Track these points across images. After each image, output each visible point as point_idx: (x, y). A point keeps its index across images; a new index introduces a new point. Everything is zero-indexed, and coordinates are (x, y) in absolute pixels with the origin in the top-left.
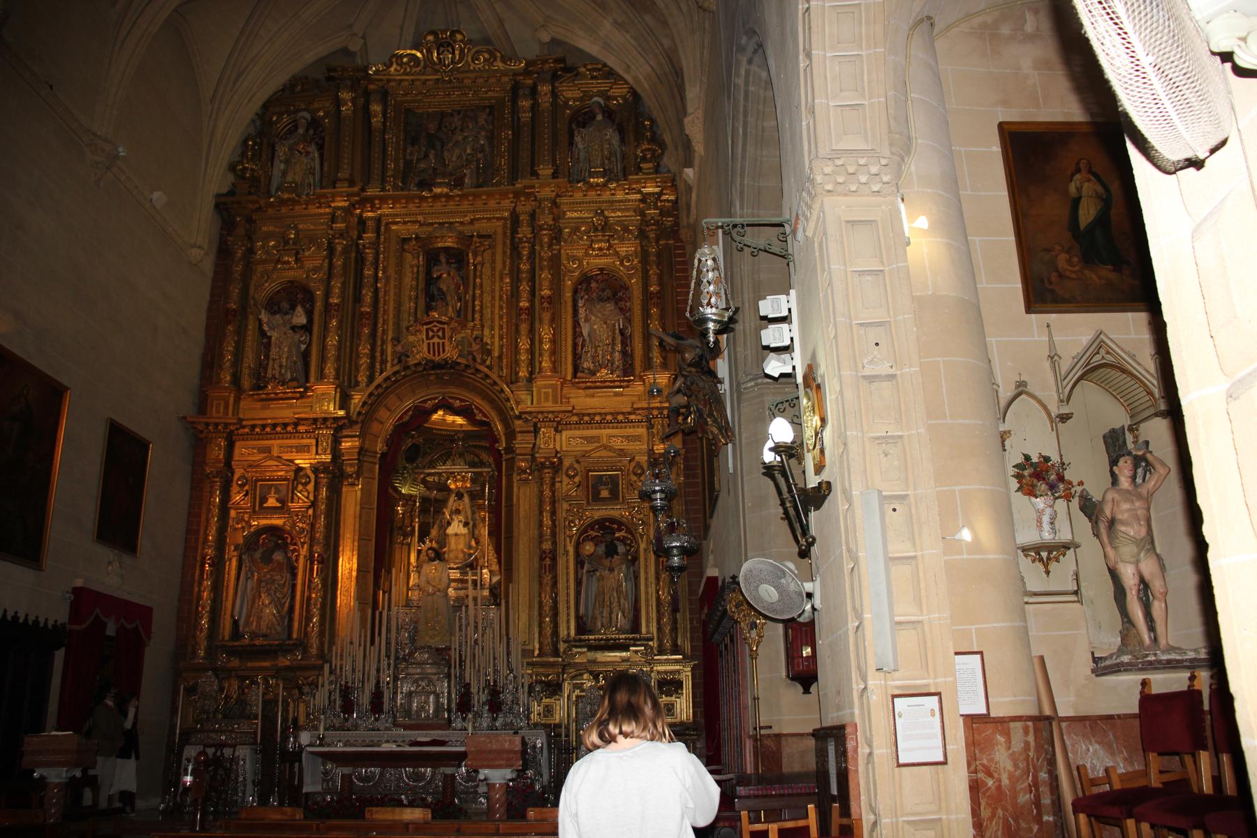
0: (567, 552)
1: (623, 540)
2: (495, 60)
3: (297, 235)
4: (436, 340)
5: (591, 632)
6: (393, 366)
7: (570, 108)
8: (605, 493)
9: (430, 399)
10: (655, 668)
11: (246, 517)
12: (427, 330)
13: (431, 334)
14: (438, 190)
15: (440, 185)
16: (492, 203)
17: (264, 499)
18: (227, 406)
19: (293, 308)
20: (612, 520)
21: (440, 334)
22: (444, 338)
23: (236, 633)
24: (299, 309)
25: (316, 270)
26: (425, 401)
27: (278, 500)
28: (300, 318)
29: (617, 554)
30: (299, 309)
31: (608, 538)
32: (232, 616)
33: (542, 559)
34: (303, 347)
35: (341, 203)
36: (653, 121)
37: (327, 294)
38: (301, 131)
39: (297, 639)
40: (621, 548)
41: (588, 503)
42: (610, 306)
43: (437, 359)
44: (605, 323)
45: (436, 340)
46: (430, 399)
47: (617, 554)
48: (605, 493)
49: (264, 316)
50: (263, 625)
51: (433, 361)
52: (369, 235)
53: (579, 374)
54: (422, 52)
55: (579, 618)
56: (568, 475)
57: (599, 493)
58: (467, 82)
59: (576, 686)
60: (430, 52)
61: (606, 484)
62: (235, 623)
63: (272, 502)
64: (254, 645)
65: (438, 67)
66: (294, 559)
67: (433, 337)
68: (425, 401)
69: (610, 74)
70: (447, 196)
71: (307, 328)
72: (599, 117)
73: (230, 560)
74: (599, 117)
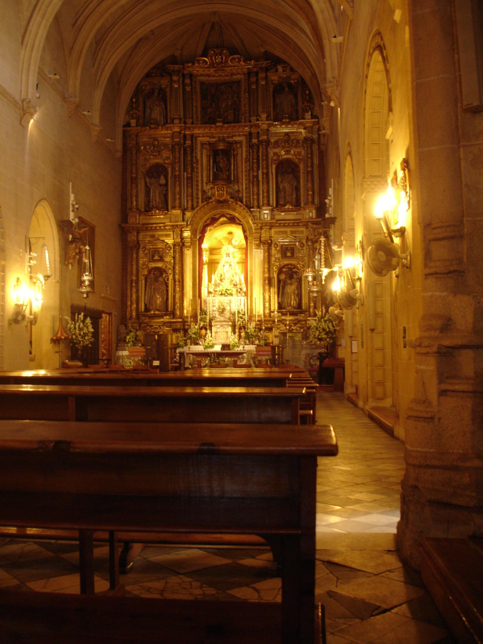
0: (274, 277)
1: (296, 273)
2: (240, 61)
3: (158, 143)
4: (221, 192)
5: (284, 308)
6: (202, 202)
7: (273, 84)
8: (289, 254)
9: (218, 214)
10: (308, 322)
11: (147, 263)
12: (217, 188)
13: (218, 189)
14: (218, 124)
15: (219, 122)
16: (241, 129)
17: (153, 256)
18: (136, 219)
19: (160, 176)
20: (291, 265)
21: (222, 189)
22: (224, 191)
23: (147, 310)
24: (162, 177)
25: (167, 158)
26: (215, 215)
27: (159, 257)
28: (163, 181)
29: (293, 278)
30: (162, 177)
31: (290, 272)
32: (145, 303)
33: (265, 280)
34: (164, 192)
35: (177, 130)
36: (310, 91)
37: (173, 170)
38: (156, 94)
39: (171, 311)
40: (295, 276)
41: (282, 258)
42: (291, 176)
43: (221, 199)
44: (289, 183)
45: (221, 192)
46: (218, 214)
47: (293, 278)
48: (289, 254)
49: (148, 180)
50: (158, 307)
51: (220, 200)
52: (188, 142)
53: (279, 206)
54: (208, 59)
55: (279, 303)
56: (274, 247)
57: (286, 254)
58: (228, 71)
59: (278, 329)
60: (211, 58)
61: (289, 251)
62: (145, 305)
63: (156, 257)
64: (155, 314)
65: (215, 65)
66: (166, 280)
67: (219, 190)
68: (215, 215)
69: (292, 70)
70: (222, 127)
71: (166, 185)
72: (286, 89)
73: (142, 281)
74: (286, 89)
